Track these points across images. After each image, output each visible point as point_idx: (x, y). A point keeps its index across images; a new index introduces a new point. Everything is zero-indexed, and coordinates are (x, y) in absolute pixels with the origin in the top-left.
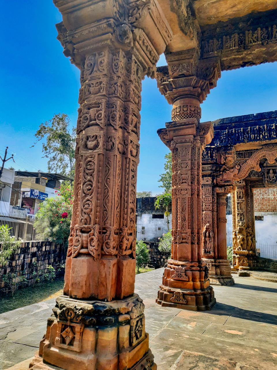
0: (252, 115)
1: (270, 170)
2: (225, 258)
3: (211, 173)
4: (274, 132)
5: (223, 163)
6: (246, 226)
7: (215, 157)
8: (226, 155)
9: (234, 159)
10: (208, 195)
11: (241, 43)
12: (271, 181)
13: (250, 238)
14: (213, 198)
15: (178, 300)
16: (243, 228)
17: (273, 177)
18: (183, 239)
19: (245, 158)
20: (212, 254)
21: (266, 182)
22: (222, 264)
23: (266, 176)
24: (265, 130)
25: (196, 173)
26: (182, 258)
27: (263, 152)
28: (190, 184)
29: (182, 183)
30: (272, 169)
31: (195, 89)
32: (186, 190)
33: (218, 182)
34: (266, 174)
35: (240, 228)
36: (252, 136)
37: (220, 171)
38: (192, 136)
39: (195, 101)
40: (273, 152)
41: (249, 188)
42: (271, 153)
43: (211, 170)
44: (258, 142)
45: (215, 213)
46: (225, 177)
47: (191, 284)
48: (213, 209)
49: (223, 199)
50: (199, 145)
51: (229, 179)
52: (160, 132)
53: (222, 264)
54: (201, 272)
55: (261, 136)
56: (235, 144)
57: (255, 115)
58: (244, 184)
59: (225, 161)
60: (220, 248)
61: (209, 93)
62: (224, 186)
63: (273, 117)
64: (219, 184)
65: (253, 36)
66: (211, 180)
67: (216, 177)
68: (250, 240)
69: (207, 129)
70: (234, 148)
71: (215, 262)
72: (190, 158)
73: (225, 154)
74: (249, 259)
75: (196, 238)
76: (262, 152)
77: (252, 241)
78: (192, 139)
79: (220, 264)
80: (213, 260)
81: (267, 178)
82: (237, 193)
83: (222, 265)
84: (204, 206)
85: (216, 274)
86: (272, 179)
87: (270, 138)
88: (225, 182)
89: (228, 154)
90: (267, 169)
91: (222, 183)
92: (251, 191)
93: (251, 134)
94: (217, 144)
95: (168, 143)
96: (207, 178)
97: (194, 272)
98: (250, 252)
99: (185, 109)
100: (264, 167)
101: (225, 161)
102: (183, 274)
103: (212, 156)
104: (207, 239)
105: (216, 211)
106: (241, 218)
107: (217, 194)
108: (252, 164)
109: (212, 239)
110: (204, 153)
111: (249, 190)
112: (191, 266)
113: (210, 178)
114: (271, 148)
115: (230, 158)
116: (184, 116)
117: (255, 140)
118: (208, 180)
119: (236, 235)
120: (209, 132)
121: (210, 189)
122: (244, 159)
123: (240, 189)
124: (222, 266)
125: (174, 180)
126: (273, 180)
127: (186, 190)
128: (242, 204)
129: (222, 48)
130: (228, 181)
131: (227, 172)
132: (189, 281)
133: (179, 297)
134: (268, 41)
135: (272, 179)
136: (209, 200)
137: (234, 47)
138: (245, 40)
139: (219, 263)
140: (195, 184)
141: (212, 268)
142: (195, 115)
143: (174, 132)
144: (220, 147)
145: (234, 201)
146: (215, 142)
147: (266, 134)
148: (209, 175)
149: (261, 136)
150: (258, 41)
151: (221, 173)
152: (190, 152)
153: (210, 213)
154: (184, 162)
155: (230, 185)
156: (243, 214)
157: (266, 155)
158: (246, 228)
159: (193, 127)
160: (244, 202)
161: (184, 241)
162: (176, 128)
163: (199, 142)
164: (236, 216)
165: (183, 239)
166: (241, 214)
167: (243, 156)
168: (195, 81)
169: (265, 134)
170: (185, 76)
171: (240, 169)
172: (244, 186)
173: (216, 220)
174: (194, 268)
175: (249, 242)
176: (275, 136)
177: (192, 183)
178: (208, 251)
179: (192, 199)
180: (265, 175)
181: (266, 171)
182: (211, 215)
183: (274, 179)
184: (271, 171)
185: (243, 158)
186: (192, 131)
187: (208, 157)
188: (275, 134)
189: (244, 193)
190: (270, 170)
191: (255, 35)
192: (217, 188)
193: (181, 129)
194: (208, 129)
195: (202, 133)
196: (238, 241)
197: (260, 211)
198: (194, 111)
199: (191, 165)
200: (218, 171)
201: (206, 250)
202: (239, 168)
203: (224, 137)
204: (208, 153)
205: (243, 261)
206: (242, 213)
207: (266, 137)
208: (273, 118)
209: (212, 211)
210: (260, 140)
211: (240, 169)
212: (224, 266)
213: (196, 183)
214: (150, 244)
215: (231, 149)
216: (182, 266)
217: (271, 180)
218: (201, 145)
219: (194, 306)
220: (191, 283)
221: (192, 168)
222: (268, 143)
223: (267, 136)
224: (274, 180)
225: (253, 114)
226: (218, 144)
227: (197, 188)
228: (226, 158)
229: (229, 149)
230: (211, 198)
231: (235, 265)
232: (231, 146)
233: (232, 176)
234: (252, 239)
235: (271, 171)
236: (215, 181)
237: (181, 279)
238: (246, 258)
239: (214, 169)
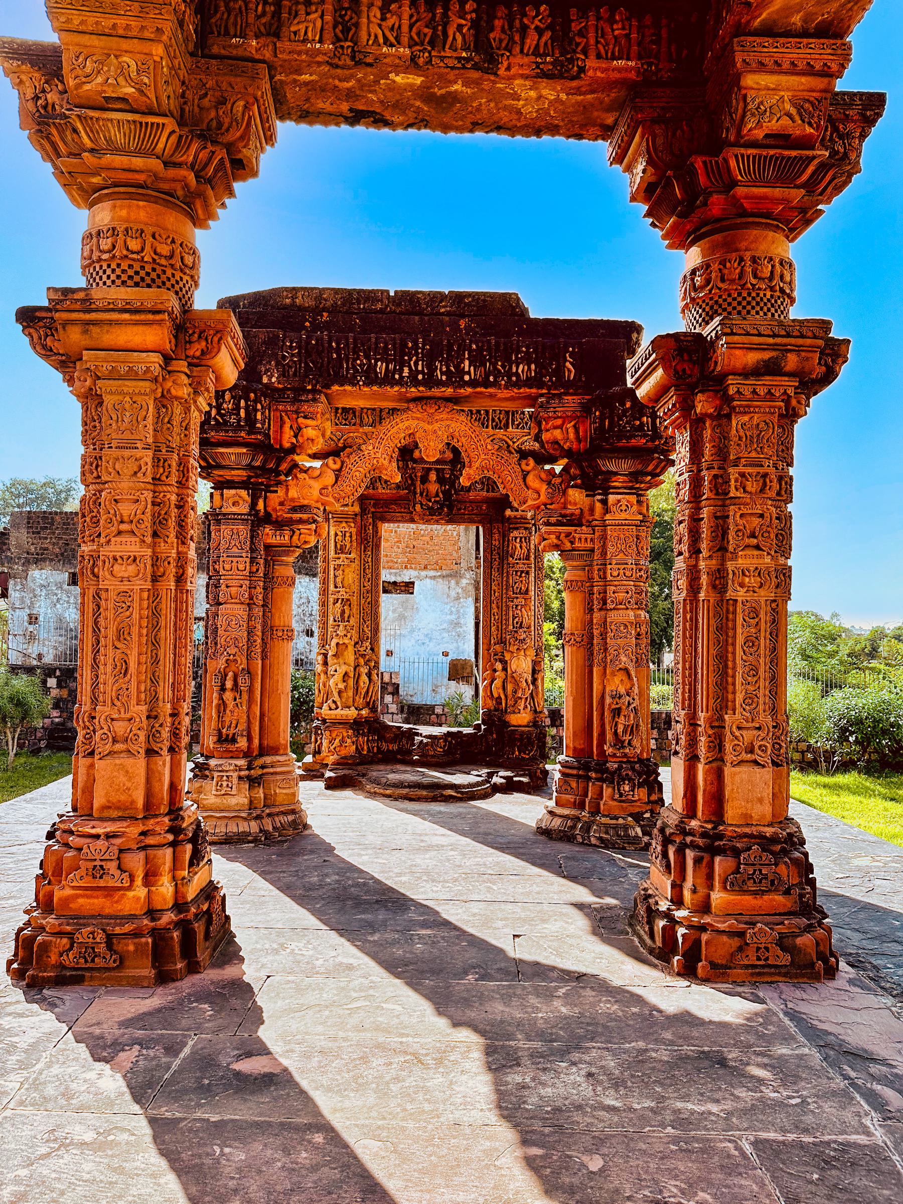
0: (382, 291)
1: (430, 469)
2: (282, 752)
3: (249, 477)
4: (441, 362)
5: (287, 445)
6: (355, 638)
7: (263, 424)
8: (301, 420)
9: (323, 436)
10: (235, 550)
11: (346, 31)
13: (364, 670)
14: (253, 560)
15: (89, 959)
16: (346, 641)
18: (115, 741)
19: (361, 425)
20: (242, 743)
22: (271, 770)
24: (417, 354)
25: (174, 498)
26: (109, 807)
27: (410, 422)
28: (149, 540)
29: (120, 533)
30: (436, 469)
31: (172, 173)
32: (135, 560)
33: (269, 509)
35: (337, 644)
36: (381, 367)
37: (278, 473)
38: (156, 358)
39: (173, 220)
40: (436, 426)
41: (371, 520)
42: (430, 427)
43: (250, 467)
44: (396, 389)
45: (258, 611)
46: (293, 493)
47: (139, 898)
48: (251, 598)
49: (287, 564)
50: (185, 391)
51: (306, 502)
52: (28, 317)
53: (271, 770)
54: (179, 848)
55: (406, 370)
56: (328, 387)
58: (357, 509)
59: (294, 440)
60: (270, 719)
61: (231, 193)
62: (290, 522)
63: (442, 310)
64: (274, 516)
65: (383, 19)
66: (249, 499)
67: (267, 491)
68: (364, 678)
69: (216, 339)
70: (323, 398)
71: (249, 768)
72: (150, 440)
73: (295, 416)
74: (357, 733)
75: (165, 733)
76: (407, 423)
77: (370, 680)
78: (156, 370)
79: (265, 770)
80: (242, 762)
81: (421, 494)
82: (336, 535)
83: (272, 774)
84: (223, 587)
85: (251, 805)
87: (430, 381)
88: (294, 510)
89: (305, 417)
91: (283, 514)
92: (376, 531)
93: (377, 361)
94: (272, 376)
95: (66, 363)
96: (233, 492)
97: (151, 852)
98: (363, 712)
99: (134, 245)
100: (415, 461)
101: (294, 440)
102: (112, 866)
103: (251, 420)
104: (228, 696)
105: (261, 603)
106: (343, 612)
107: (268, 547)
108: (378, 456)
109: (245, 696)
110: (225, 406)
112: (143, 833)
113: (243, 493)
114: (432, 411)
115: (310, 432)
116: (131, 272)
117: (388, 380)
118: (237, 499)
120: (223, 347)
121: (244, 530)
123: (344, 524)
124: (272, 778)
125: (88, 519)
127: (135, 560)
128: (347, 571)
129: (277, 35)
130: (303, 508)
131: (301, 476)
132: (130, 888)
133: (93, 948)
134: (430, 53)
136: (241, 567)
137: (320, 41)
138: (357, 25)
139: (263, 767)
140: (169, 541)
141: (239, 790)
142: (173, 275)
143: (85, 332)
144: (277, 389)
145: (326, 560)
146: (263, 369)
147: (420, 368)
149: (406, 370)
150: (399, 43)
151: (283, 477)
152: (150, 419)
153: (240, 611)
154: (127, 453)
155: (307, 522)
156: (348, 600)
157: (417, 435)
158: (356, 643)
159: (160, 323)
160: (353, 565)
161: (119, 747)
162: (93, 316)
163: (186, 380)
164: (331, 606)
165: (115, 741)
166: (347, 602)
168: (174, 138)
169: (416, 364)
170: (133, 111)
171: (340, 470)
172: (356, 515)
173: (260, 634)
174: (150, 840)
175: (362, 684)
176: (444, 378)
177: (155, 535)
178: (227, 735)
179: (155, 595)
180: (415, 486)
182: (245, 617)
184: (433, 476)
185: (357, 427)
186: (157, 336)
187: (239, 421)
188: (444, 369)
189: (354, 538)
190: (430, 469)
191: (392, 20)
192: (267, 530)
193: (110, 323)
194: (220, 339)
195: (196, 349)
197: (406, 567)
198: (171, 257)
199: (156, 465)
200: (271, 471)
201: (224, 731)
202: (337, 467)
203: (293, 355)
204: (237, 408)
205: (343, 741)
206: (346, 597)
207: (420, 377)
208: (443, 314)
209: (248, 604)
210: (401, 382)
211: (340, 470)
212: (278, 777)
213: (172, 535)
214: (58, 673)
215: (315, 400)
216: (108, 836)
218: (196, 393)
219: (148, 972)
220: (141, 892)
221: (159, 479)
222: (426, 394)
223: (422, 372)
225: (388, 292)
226: (274, 380)
227: (178, 553)
228: (300, 429)
230: (248, 560)
231: (319, 752)
232: (314, 391)
233: (316, 493)
234: (369, 675)
235: (433, 476)
236: (261, 505)
237: (102, 883)
238: (351, 732)
239: (258, 464)
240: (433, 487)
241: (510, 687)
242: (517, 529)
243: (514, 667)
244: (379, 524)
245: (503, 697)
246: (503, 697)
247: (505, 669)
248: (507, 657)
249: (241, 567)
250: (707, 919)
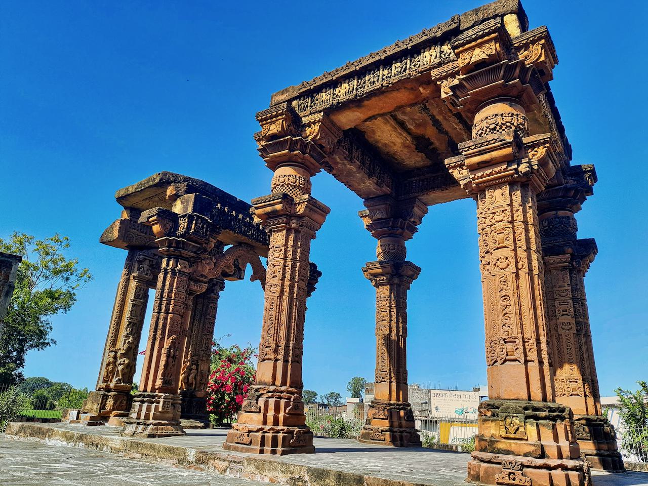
10: (181, 288)
57: (238, 200)
76: (241, 251)
119: (115, 358)
143: (310, 211)
148: (187, 258)
162: (314, 208)
169: (254, 232)
196: (120, 368)
229: (217, 232)
241: (198, 378)
242: (213, 303)
243: (202, 368)
245: (194, 383)
246: (194, 383)
247: (197, 369)
248: (200, 362)
249: (182, 297)
250: (403, 429)
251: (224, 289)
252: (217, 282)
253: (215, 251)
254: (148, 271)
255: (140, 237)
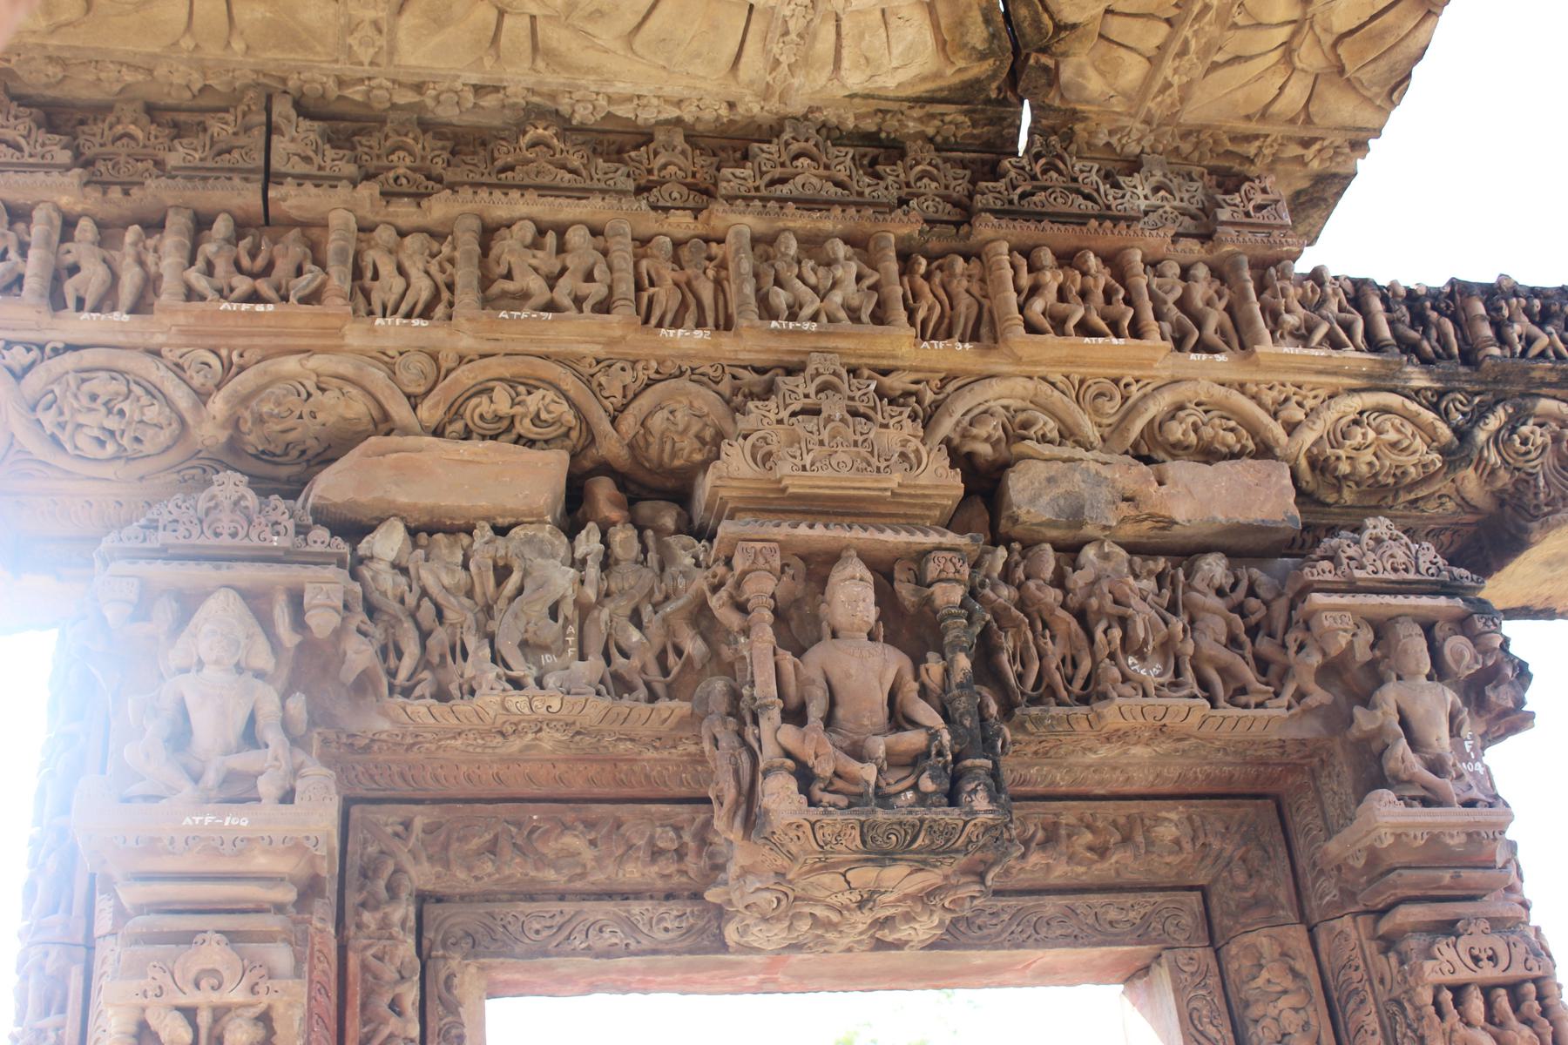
1: (818, 567)
12: (869, 772)
17: (898, 719)
21: (780, 794)
23: (764, 687)
34: (760, 648)
86: (879, 746)
90: (784, 546)
111: (410, 995)
122: (355, 335)
123: (214, 953)
126: (894, 760)
135: (879, 746)
167: (339, 278)
181: (762, 588)
183: (912, 740)
184: (852, 597)
217: (858, 753)
224: (915, 762)
240: (866, 668)
242: (1449, 928)
244: (468, 977)
251: (1534, 699)
252: (1382, 629)
253: (1185, 273)
254: (250, 737)
255: (70, 360)
